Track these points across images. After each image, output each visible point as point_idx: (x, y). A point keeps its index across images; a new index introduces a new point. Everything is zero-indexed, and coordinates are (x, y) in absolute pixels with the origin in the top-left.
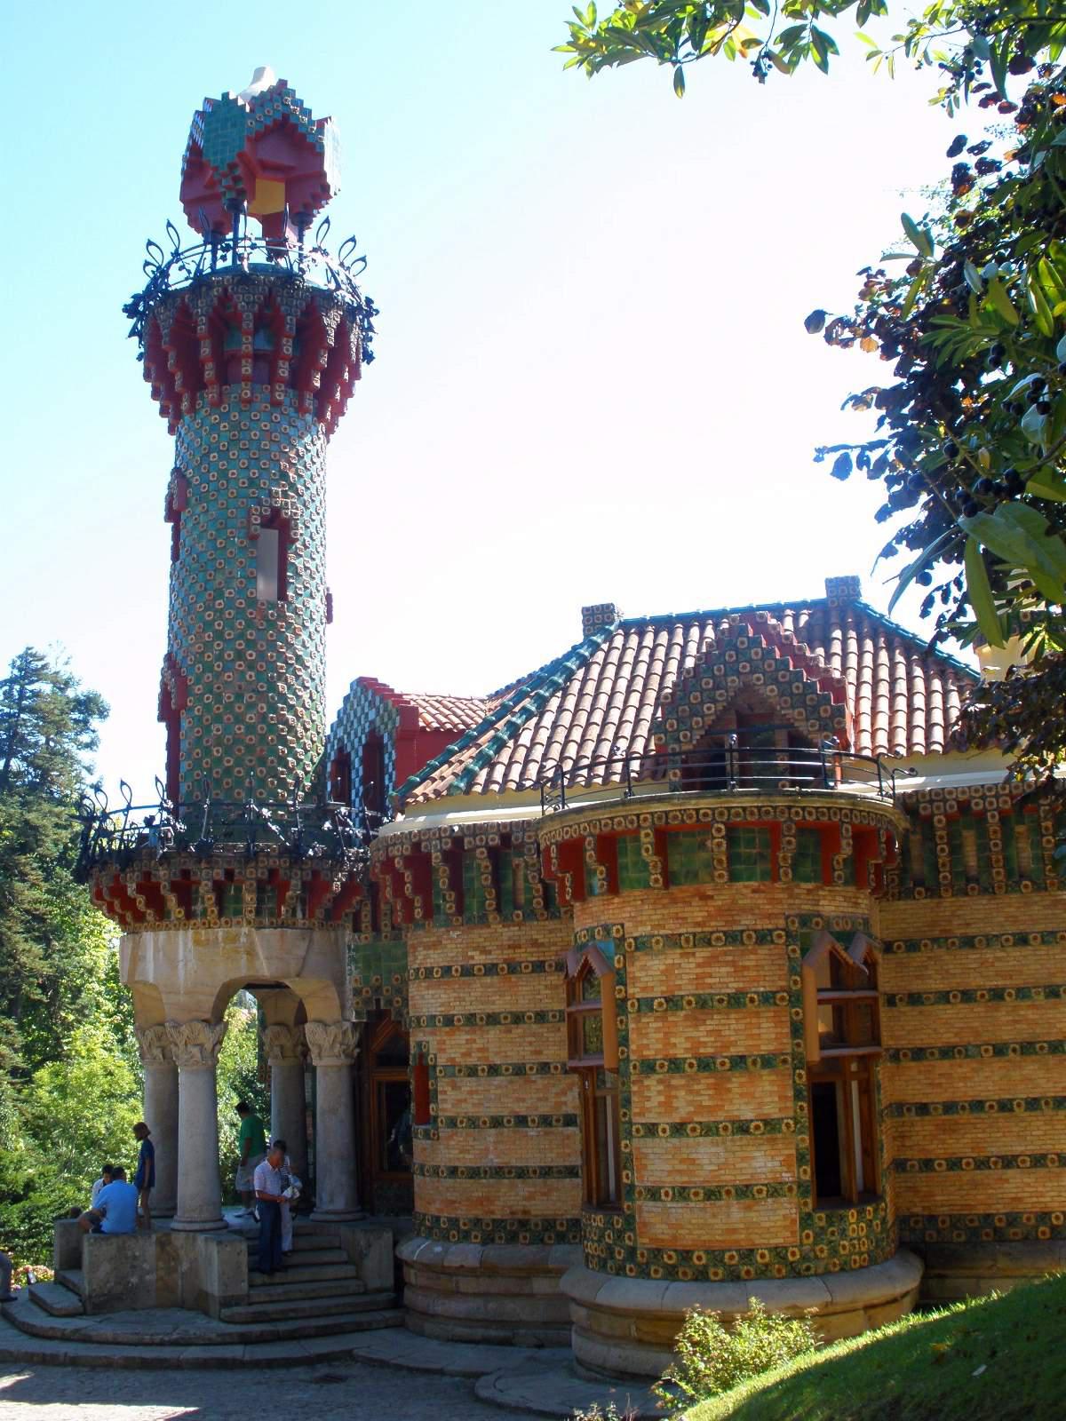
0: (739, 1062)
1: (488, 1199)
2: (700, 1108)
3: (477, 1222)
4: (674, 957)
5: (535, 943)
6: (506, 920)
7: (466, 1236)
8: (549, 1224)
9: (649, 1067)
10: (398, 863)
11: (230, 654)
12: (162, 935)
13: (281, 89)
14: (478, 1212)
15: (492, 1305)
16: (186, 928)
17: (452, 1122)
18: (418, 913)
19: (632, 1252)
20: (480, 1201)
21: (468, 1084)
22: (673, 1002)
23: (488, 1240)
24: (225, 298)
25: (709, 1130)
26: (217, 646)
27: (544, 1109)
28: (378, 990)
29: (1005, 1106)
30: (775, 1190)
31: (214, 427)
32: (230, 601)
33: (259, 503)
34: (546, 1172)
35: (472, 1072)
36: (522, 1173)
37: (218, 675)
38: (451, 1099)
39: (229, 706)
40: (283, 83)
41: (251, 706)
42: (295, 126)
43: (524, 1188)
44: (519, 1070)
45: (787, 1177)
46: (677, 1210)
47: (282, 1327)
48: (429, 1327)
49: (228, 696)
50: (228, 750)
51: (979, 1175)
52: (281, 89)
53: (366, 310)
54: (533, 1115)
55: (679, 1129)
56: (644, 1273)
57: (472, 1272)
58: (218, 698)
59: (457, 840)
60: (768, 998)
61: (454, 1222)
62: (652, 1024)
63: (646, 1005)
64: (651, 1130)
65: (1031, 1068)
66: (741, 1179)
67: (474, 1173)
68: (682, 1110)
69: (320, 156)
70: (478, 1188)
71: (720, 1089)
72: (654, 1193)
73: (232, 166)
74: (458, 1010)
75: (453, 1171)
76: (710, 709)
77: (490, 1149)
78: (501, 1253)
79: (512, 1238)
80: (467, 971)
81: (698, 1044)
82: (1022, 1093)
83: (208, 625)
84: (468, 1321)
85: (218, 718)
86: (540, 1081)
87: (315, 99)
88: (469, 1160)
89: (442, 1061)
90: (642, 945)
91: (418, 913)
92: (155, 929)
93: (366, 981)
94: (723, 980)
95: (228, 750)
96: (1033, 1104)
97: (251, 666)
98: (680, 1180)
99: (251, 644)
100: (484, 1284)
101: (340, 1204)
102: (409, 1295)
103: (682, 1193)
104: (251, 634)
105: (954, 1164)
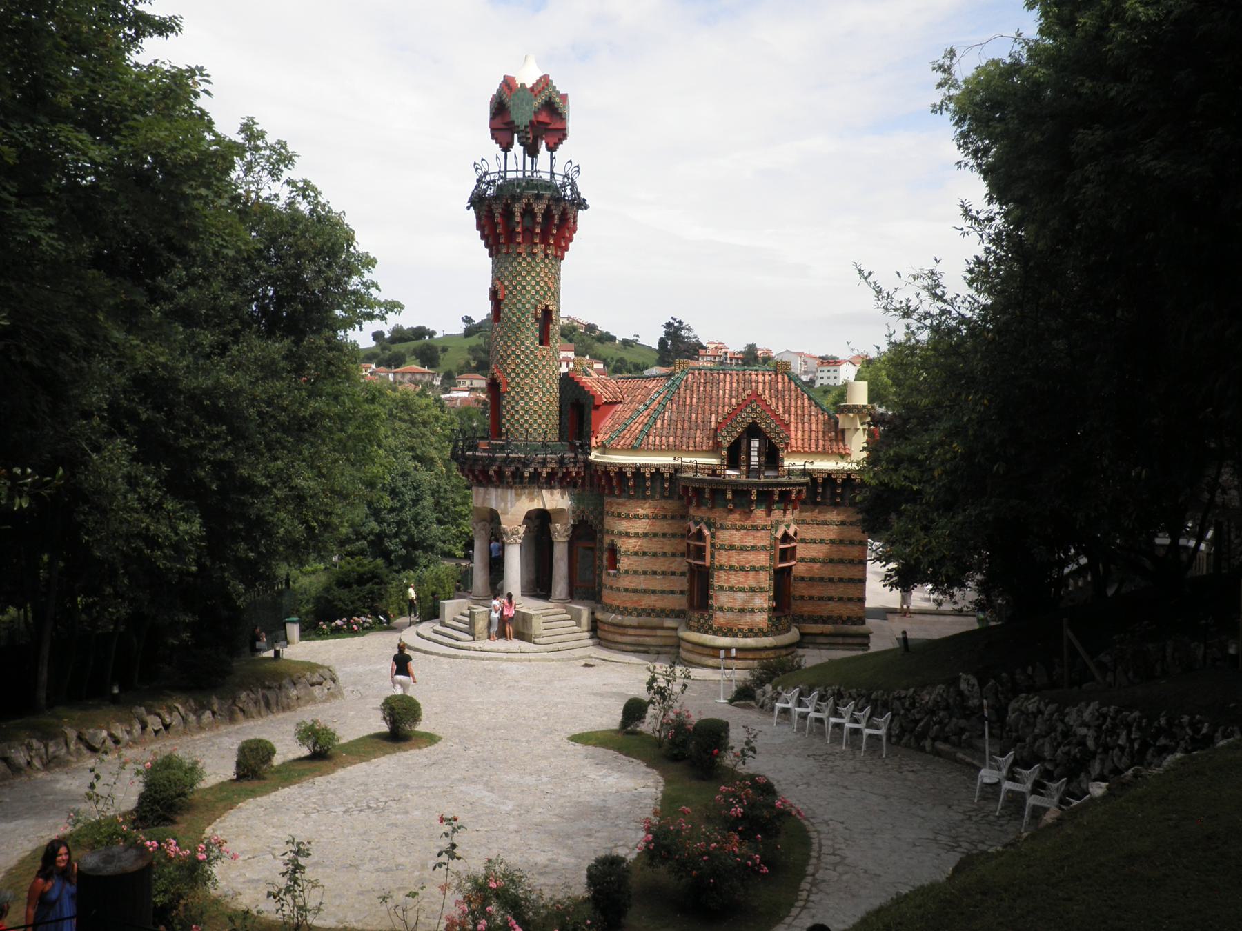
0: (754, 569)
1: (640, 601)
2: (739, 582)
3: (635, 609)
4: (734, 532)
5: (663, 508)
6: (652, 497)
7: (630, 614)
8: (663, 611)
9: (721, 567)
10: (612, 474)
11: (527, 370)
12: (500, 490)
13: (544, 83)
14: (636, 605)
15: (641, 639)
16: (511, 487)
17: (627, 572)
18: (617, 493)
19: (711, 627)
20: (637, 601)
21: (633, 558)
22: (732, 547)
23: (639, 615)
24: (528, 205)
25: (742, 590)
26: (522, 366)
27: (663, 569)
28: (583, 511)
29: (831, 580)
30: (761, 610)
31: (520, 264)
32: (527, 347)
33: (540, 302)
34: (663, 592)
35: (636, 554)
36: (654, 592)
37: (522, 379)
38: (624, 564)
39: (527, 394)
40: (546, 77)
41: (536, 393)
42: (553, 104)
43: (654, 597)
44: (655, 554)
45: (765, 606)
46: (729, 615)
47: (560, 646)
48: (613, 645)
49: (527, 389)
50: (527, 412)
51: (819, 602)
52: (545, 82)
53: (582, 204)
54: (659, 571)
55: (731, 589)
56: (715, 633)
57: (631, 627)
58: (522, 389)
59: (638, 468)
60: (764, 548)
61: (625, 609)
62: (723, 553)
63: (722, 547)
64: (721, 588)
65: (841, 567)
66: (751, 605)
67: (635, 591)
68: (733, 582)
69: (565, 119)
70: (635, 597)
71: (746, 577)
72: (721, 609)
73: (526, 127)
74: (632, 531)
75: (626, 590)
76: (740, 430)
77: (641, 583)
78: (643, 620)
79: (649, 615)
80: (637, 517)
81: (739, 561)
82: (836, 577)
83: (518, 357)
84: (631, 644)
85: (522, 398)
86: (662, 559)
87: (561, 86)
88: (633, 586)
89: (623, 549)
90: (722, 527)
91: (617, 493)
92: (497, 487)
93: (578, 508)
94: (750, 540)
95: (527, 412)
96: (841, 580)
97: (536, 376)
98: (729, 605)
99: (536, 366)
100: (639, 632)
101: (563, 596)
102: (600, 633)
103: (731, 610)
104: (536, 362)
105: (811, 598)
